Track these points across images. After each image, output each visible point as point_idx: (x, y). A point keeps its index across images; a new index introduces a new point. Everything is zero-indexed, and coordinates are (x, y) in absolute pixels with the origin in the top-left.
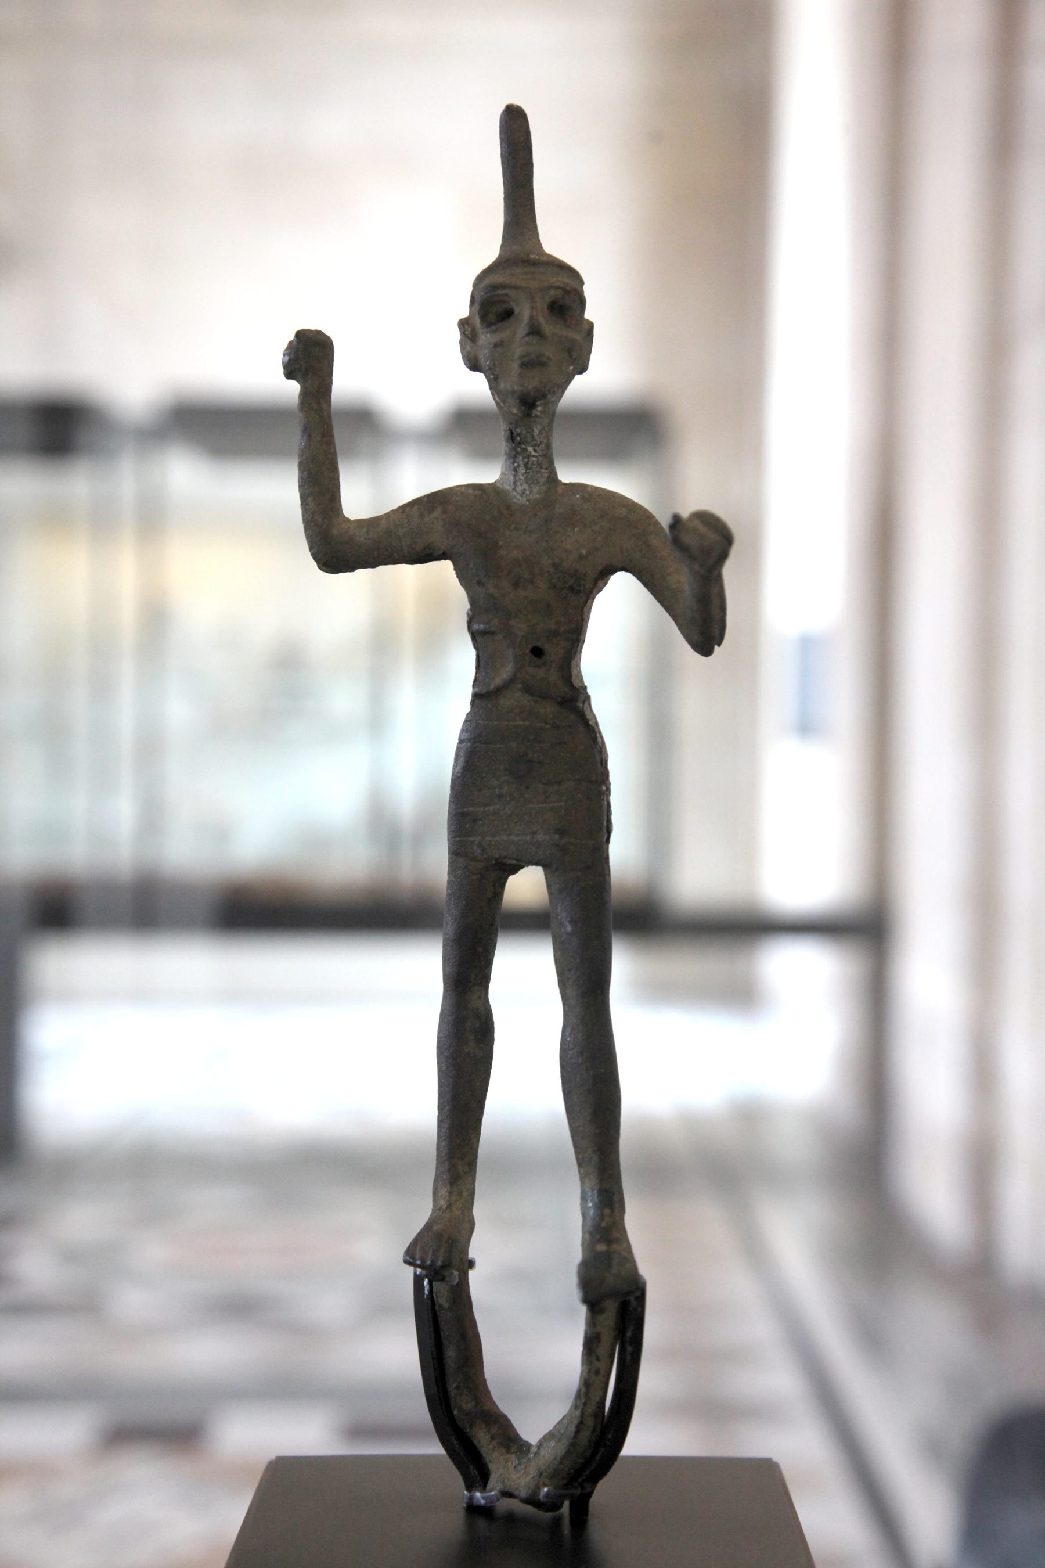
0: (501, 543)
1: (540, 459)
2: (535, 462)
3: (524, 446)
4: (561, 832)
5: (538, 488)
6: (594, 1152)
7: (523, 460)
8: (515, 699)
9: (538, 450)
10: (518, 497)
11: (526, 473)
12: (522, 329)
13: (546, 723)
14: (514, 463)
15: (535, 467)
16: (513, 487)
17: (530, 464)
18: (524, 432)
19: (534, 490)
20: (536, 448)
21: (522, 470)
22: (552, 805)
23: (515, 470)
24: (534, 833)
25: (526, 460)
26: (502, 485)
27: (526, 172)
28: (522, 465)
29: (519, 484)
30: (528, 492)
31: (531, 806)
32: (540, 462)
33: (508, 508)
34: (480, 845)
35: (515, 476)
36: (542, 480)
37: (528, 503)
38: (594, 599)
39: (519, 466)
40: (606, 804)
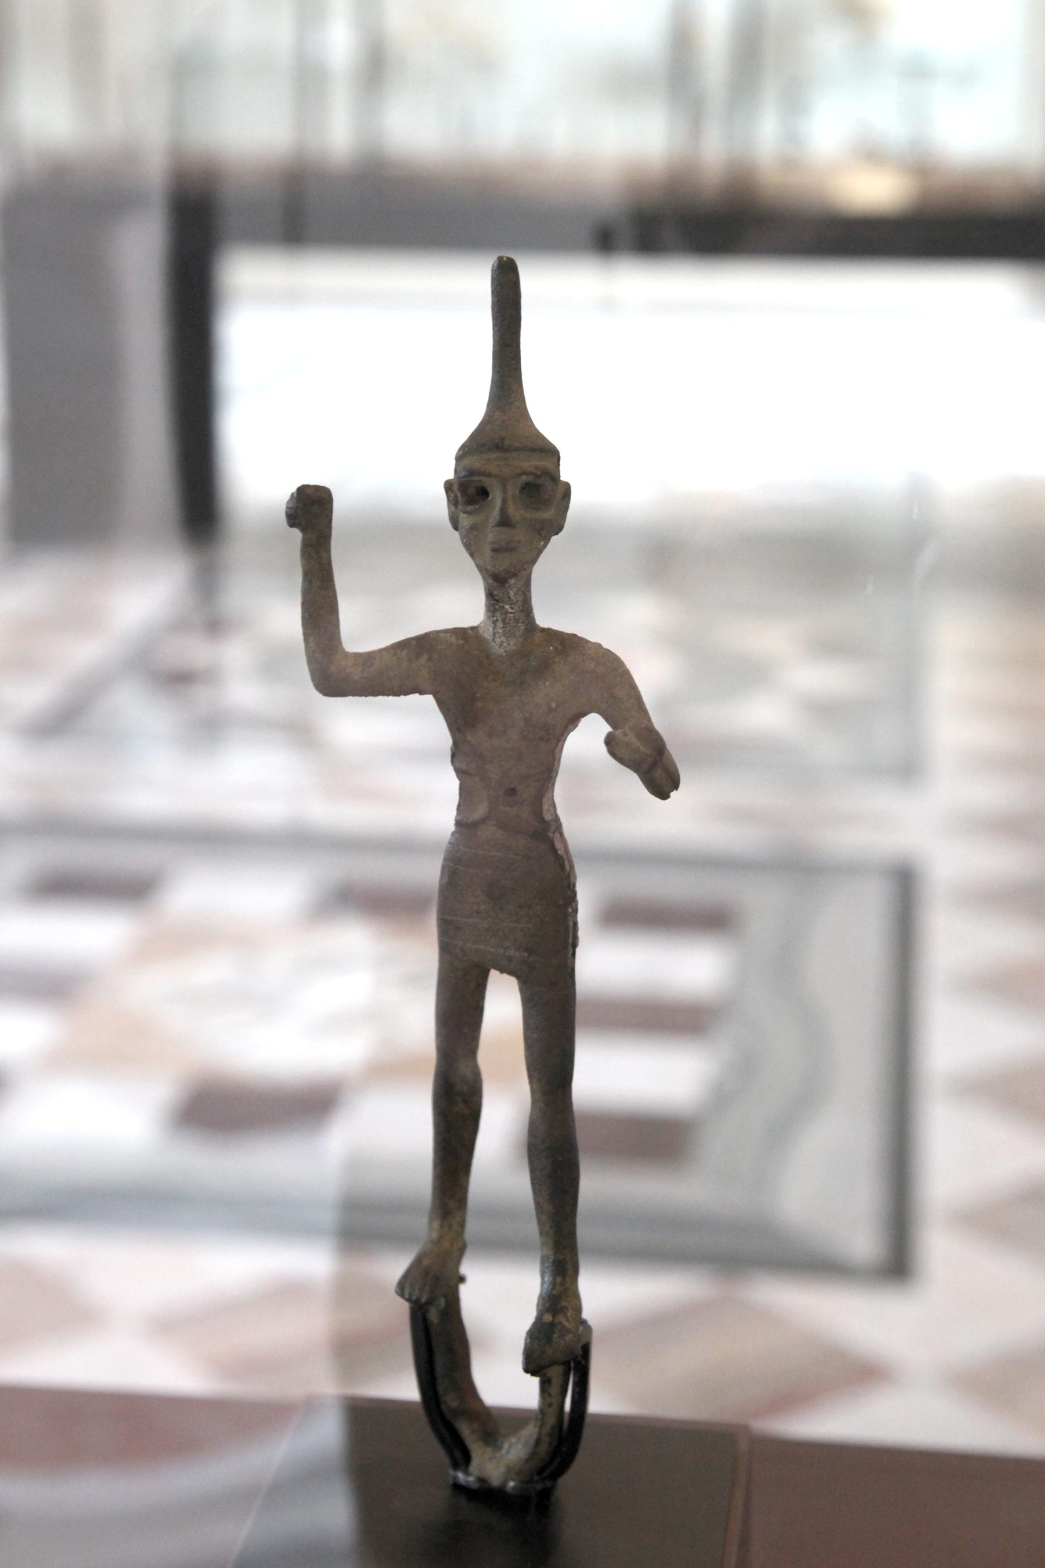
0: (478, 695)
1: (517, 614)
2: (512, 618)
3: (501, 605)
4: (530, 951)
5: (514, 640)
6: (551, 1227)
7: (500, 616)
8: (489, 832)
9: (514, 608)
10: (497, 647)
11: (503, 627)
12: (495, 514)
13: (518, 855)
14: (493, 617)
15: (512, 622)
16: (492, 638)
17: (507, 620)
18: (500, 594)
19: (511, 643)
20: (513, 606)
21: (500, 624)
22: (521, 926)
23: (494, 622)
24: (506, 948)
25: (504, 616)
26: (484, 632)
27: (513, 330)
28: (500, 620)
29: (497, 636)
30: (505, 644)
31: (505, 924)
32: (517, 617)
33: (488, 657)
34: (462, 950)
35: (494, 628)
36: (518, 634)
37: (505, 654)
38: (565, 740)
39: (497, 620)
40: (571, 924)
